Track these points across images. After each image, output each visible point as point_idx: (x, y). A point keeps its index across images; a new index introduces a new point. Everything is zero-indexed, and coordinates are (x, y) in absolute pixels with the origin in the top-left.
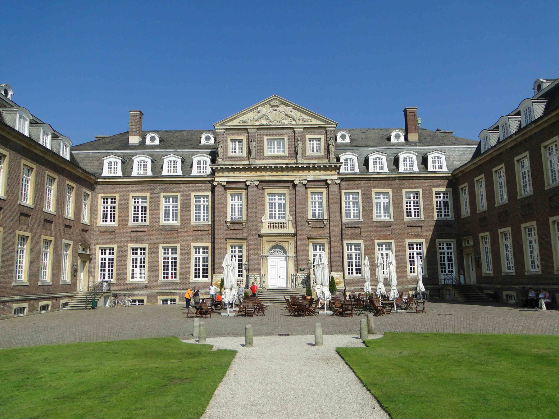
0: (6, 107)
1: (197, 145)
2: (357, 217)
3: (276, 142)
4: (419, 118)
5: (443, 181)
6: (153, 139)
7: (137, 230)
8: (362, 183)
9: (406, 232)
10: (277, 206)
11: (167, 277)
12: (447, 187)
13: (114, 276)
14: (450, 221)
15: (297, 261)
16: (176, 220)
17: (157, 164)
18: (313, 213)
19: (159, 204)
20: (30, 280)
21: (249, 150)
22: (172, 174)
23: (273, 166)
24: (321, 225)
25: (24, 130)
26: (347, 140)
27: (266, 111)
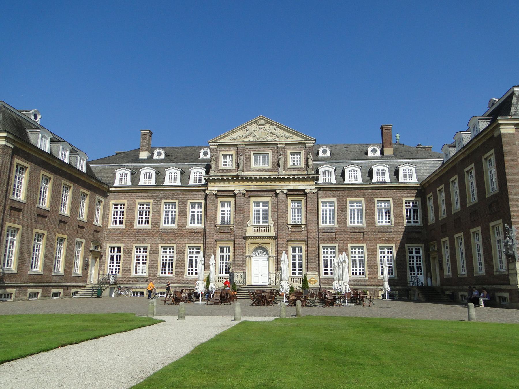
0: (32, 128)
1: (196, 159)
2: (333, 222)
3: (261, 157)
4: (398, 135)
5: (412, 191)
6: (159, 154)
7: (141, 232)
8: (337, 193)
9: (377, 237)
10: (261, 212)
11: (165, 273)
12: (416, 197)
13: (121, 271)
14: (419, 227)
16: (174, 223)
17: (160, 175)
18: (292, 219)
19: (160, 210)
20: (44, 270)
21: (238, 163)
22: (173, 184)
23: (258, 177)
24: (300, 229)
25: (45, 147)
26: (328, 154)
27: (253, 129)
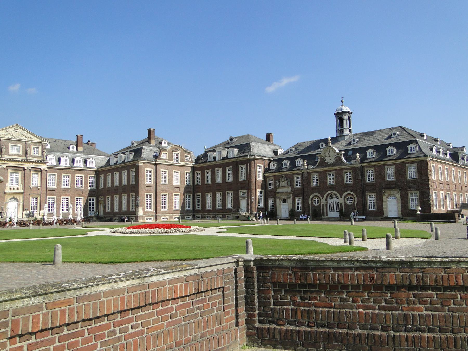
10: (14, 179)
15: (24, 205)
24: (37, 189)
